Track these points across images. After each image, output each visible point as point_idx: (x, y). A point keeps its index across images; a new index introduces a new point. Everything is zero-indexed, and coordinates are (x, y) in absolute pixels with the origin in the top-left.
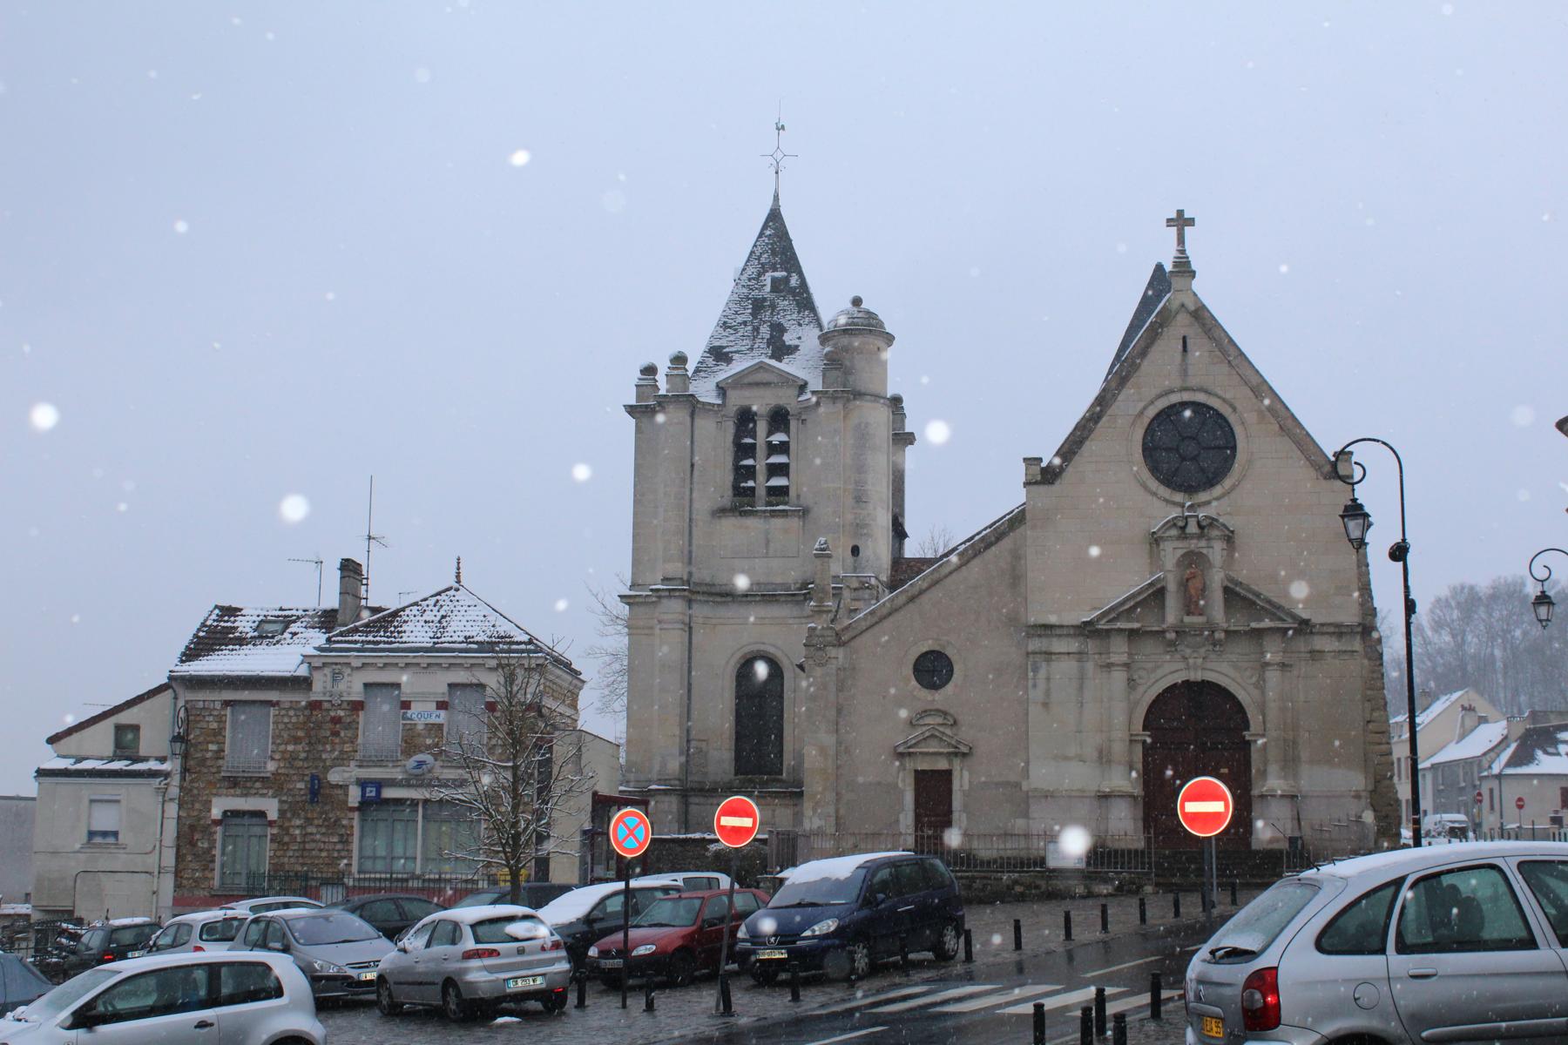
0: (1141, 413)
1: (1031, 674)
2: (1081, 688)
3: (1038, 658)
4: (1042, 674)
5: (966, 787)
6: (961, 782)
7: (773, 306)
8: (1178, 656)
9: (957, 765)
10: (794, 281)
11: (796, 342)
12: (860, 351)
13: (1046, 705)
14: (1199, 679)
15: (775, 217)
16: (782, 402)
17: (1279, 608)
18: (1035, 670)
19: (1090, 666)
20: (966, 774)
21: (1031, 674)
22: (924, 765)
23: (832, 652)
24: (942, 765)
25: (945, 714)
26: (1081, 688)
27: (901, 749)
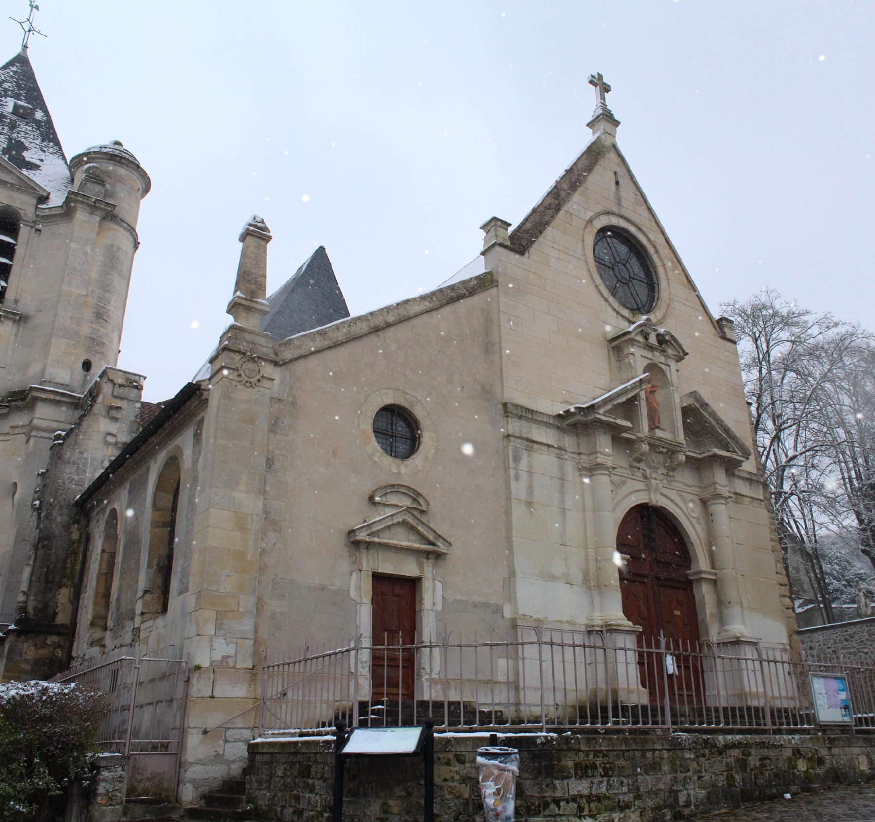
0: (590, 221)
1: (512, 464)
2: (562, 490)
3: (518, 443)
4: (524, 464)
5: (439, 607)
6: (432, 598)
7: (13, 126)
8: (639, 474)
9: (428, 572)
10: (39, 115)
11: (38, 163)
12: (119, 179)
13: (529, 504)
14: (660, 504)
15: (21, 61)
16: (16, 205)
17: (733, 438)
18: (517, 459)
19: (569, 467)
20: (439, 586)
21: (512, 464)
22: (389, 566)
23: (268, 369)
24: (408, 568)
25: (415, 496)
26: (562, 490)
27: (362, 536)
